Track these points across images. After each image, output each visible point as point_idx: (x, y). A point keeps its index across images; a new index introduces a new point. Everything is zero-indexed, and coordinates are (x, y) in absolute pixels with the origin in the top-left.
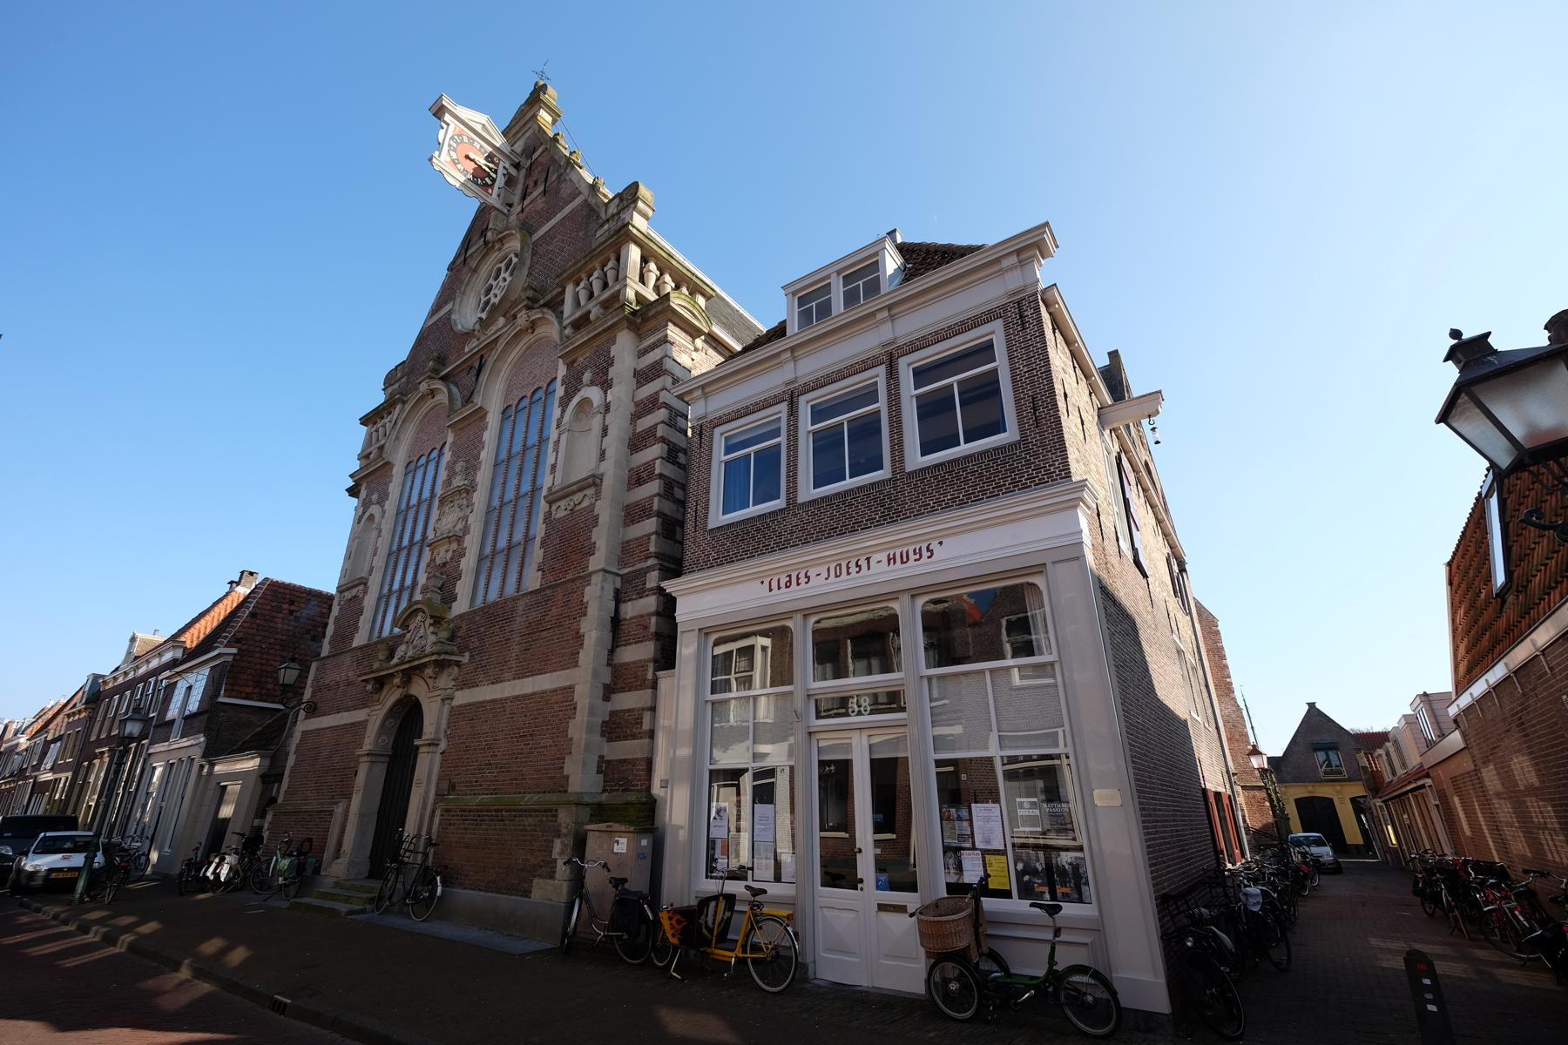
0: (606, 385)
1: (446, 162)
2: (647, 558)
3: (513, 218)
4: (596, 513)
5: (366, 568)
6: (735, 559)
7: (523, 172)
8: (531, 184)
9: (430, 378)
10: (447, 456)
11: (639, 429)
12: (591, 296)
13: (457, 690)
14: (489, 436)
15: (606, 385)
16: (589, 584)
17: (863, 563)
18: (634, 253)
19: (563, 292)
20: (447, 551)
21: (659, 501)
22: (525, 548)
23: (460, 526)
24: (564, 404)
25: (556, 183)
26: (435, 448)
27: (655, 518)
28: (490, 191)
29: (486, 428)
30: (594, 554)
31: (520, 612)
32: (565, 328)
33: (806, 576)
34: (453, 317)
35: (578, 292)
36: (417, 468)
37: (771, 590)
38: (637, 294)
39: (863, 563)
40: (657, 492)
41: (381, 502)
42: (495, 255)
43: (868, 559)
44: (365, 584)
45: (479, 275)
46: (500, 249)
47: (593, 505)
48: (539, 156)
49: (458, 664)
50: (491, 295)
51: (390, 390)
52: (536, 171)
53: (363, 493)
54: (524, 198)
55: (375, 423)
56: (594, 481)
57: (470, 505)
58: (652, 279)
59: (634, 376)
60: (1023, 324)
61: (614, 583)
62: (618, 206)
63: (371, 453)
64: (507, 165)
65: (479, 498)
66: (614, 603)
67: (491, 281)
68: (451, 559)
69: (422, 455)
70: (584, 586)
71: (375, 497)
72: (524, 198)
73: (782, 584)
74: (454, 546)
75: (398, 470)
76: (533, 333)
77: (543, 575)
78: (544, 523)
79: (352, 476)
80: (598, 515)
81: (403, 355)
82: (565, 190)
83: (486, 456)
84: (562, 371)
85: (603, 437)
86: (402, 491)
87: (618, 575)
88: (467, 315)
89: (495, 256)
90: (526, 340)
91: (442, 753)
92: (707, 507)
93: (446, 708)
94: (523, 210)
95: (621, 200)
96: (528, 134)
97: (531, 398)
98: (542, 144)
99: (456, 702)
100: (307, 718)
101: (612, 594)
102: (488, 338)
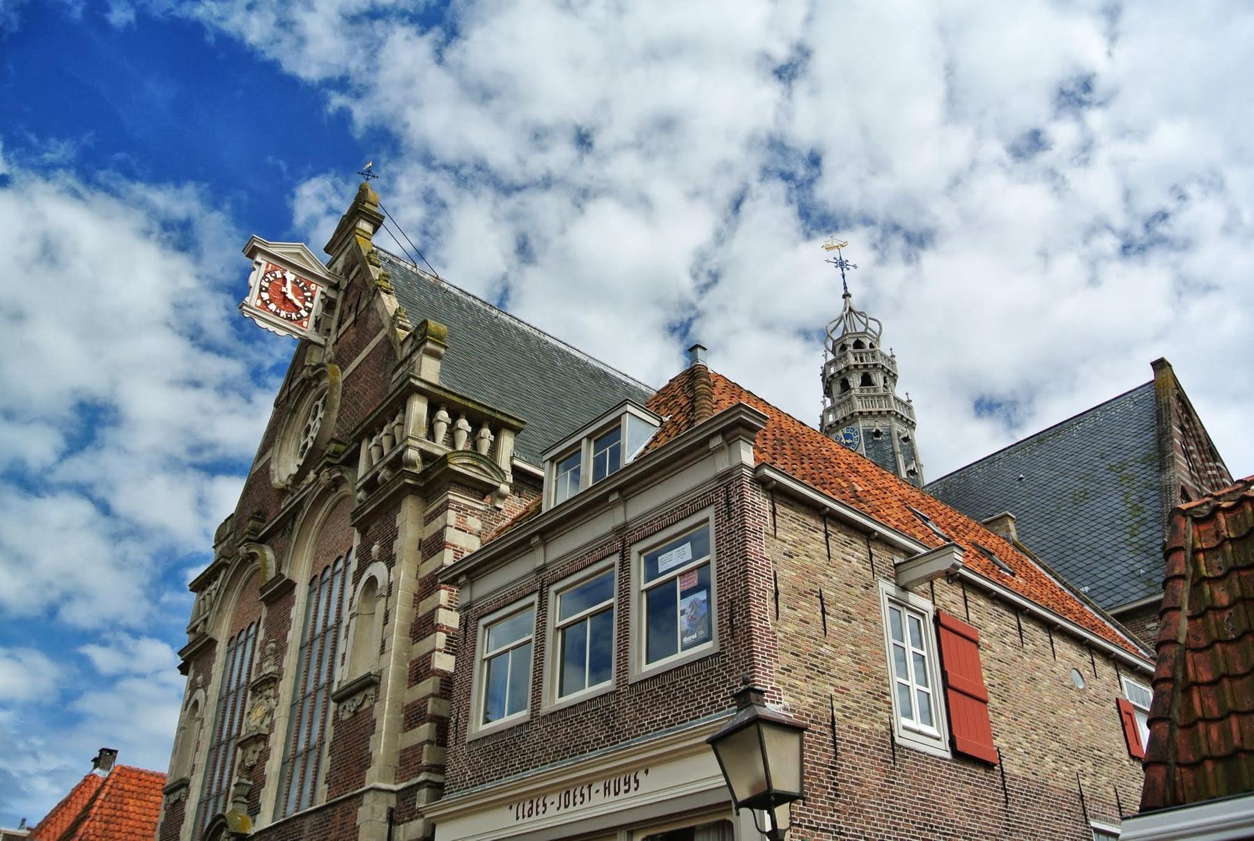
0: (390, 561)
2: (419, 773)
3: (329, 349)
4: (374, 717)
5: (189, 767)
6: (486, 780)
7: (342, 294)
8: (346, 309)
9: (248, 540)
10: (261, 636)
11: (421, 614)
12: (382, 455)
15: (390, 561)
16: (361, 805)
17: (586, 791)
18: (418, 408)
20: (254, 752)
21: (434, 702)
22: (319, 752)
23: (267, 721)
24: (356, 581)
25: (365, 311)
26: (243, 630)
27: (428, 724)
28: (305, 324)
29: (293, 604)
30: (370, 767)
31: (306, 832)
32: (358, 491)
33: (545, 805)
34: (272, 467)
35: (370, 449)
36: (237, 645)
37: (518, 818)
38: (422, 452)
39: (586, 791)
40: (431, 692)
41: (205, 685)
42: (314, 390)
43: (590, 787)
45: (299, 414)
46: (316, 386)
47: (372, 706)
48: (355, 277)
50: (309, 439)
51: (219, 548)
52: (352, 294)
53: (192, 672)
54: (339, 327)
55: (204, 589)
56: (370, 683)
57: (276, 696)
58: (441, 430)
59: (419, 549)
60: (729, 513)
61: (388, 802)
62: (412, 345)
63: (197, 626)
64: (325, 289)
65: (286, 687)
66: (387, 826)
67: (310, 422)
68: (258, 761)
69: (243, 630)
70: (358, 807)
71: (200, 678)
72: (339, 327)
73: (526, 814)
74: (261, 746)
75: (221, 648)
76: (337, 491)
77: (329, 788)
78: (333, 724)
79: (180, 653)
80: (375, 720)
82: (371, 324)
83: (294, 637)
84: (356, 541)
85: (385, 624)
86: (224, 672)
87: (392, 792)
88: (286, 466)
89: (313, 393)
90: (330, 499)
92: (467, 716)
94: (337, 340)
95: (415, 337)
96: (348, 249)
97: (322, 577)
98: (357, 263)
101: (385, 815)
102: (301, 493)
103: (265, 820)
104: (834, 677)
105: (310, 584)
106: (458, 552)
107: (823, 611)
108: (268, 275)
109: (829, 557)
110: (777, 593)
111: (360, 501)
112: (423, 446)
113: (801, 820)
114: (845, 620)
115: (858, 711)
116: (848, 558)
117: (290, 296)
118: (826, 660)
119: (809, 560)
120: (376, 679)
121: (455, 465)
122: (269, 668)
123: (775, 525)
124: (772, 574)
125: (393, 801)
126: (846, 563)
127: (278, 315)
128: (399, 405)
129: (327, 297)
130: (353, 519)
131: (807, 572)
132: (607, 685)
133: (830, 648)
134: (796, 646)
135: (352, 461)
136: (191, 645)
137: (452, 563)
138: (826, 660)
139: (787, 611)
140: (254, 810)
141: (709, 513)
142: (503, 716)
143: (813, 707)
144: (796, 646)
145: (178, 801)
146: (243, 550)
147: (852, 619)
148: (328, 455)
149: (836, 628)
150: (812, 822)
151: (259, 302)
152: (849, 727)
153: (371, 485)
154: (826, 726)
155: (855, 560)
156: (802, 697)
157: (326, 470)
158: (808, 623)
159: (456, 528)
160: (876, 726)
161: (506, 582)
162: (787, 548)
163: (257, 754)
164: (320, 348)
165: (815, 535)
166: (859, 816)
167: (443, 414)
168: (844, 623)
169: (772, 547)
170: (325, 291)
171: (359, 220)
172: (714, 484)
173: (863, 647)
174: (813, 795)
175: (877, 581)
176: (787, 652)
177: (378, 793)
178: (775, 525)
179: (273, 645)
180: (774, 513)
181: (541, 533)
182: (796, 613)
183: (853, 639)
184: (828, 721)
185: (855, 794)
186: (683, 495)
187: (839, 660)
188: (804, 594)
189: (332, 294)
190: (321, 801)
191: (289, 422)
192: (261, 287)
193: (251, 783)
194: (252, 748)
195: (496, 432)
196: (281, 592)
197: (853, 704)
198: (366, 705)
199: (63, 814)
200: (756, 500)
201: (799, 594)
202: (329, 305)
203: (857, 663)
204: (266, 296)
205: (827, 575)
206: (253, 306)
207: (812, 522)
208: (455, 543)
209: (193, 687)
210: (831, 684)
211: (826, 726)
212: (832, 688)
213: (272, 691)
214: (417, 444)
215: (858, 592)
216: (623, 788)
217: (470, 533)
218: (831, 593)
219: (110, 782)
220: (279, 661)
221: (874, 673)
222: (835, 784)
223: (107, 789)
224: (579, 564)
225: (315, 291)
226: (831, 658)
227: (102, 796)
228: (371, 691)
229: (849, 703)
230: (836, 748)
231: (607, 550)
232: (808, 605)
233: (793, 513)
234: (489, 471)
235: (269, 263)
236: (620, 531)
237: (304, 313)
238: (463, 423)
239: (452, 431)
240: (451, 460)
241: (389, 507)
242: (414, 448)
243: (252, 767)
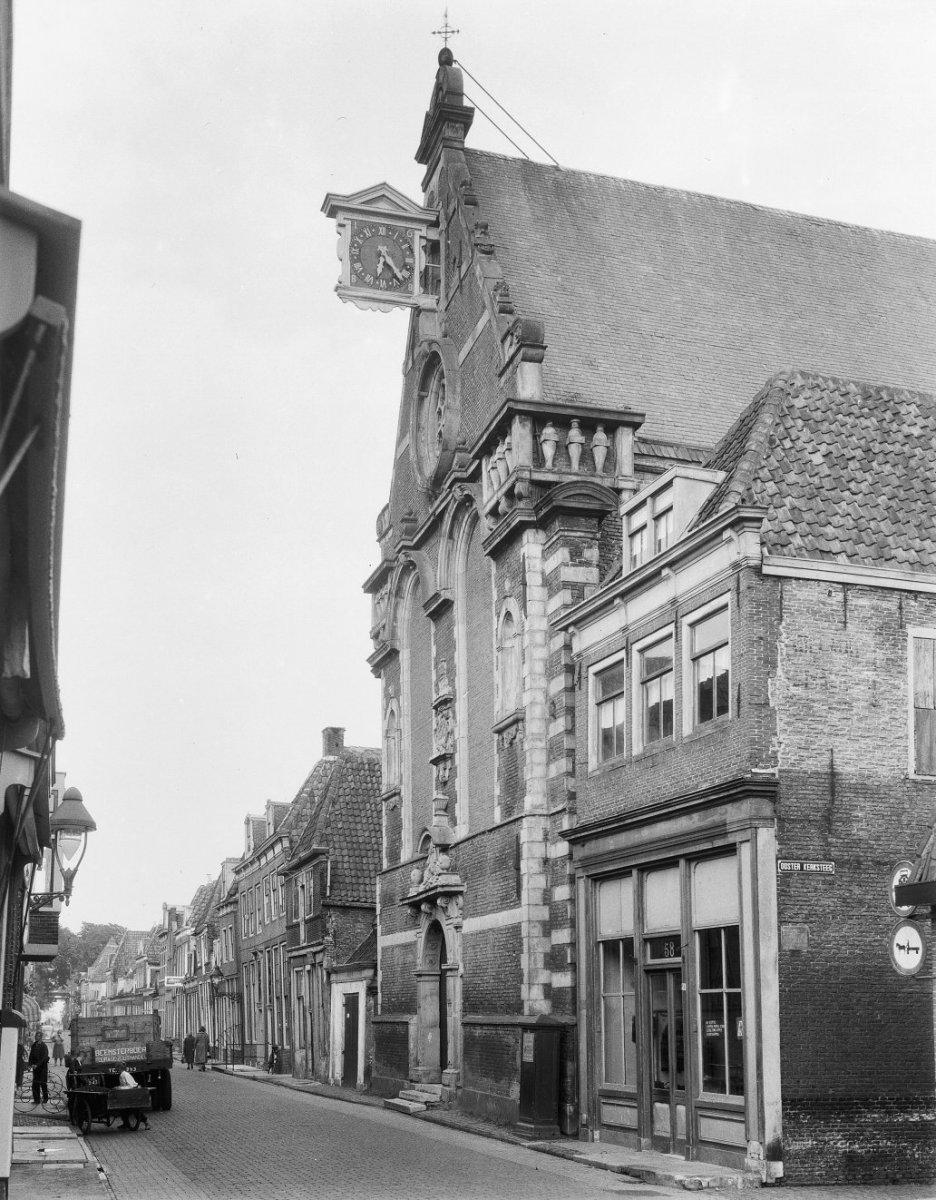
19: (480, 465)
20: (445, 769)
23: (450, 741)
38: (535, 483)
44: (399, 794)
51: (383, 541)
64: (424, 231)
65: (461, 706)
74: (449, 764)
79: (369, 660)
81: (384, 497)
103: (461, 832)
106: (577, 589)
122: (445, 691)
128: (502, 431)
129: (428, 240)
135: (476, 476)
136: (378, 652)
140: (454, 821)
141: (727, 598)
146: (402, 557)
153: (494, 512)
163: (447, 771)
170: (424, 233)
179: (445, 665)
181: (622, 595)
189: (433, 235)
194: (441, 766)
196: (440, 610)
202: (433, 248)
204: (358, 266)
209: (388, 697)
220: (452, 682)
238: (575, 434)
241: (514, 536)
243: (445, 783)
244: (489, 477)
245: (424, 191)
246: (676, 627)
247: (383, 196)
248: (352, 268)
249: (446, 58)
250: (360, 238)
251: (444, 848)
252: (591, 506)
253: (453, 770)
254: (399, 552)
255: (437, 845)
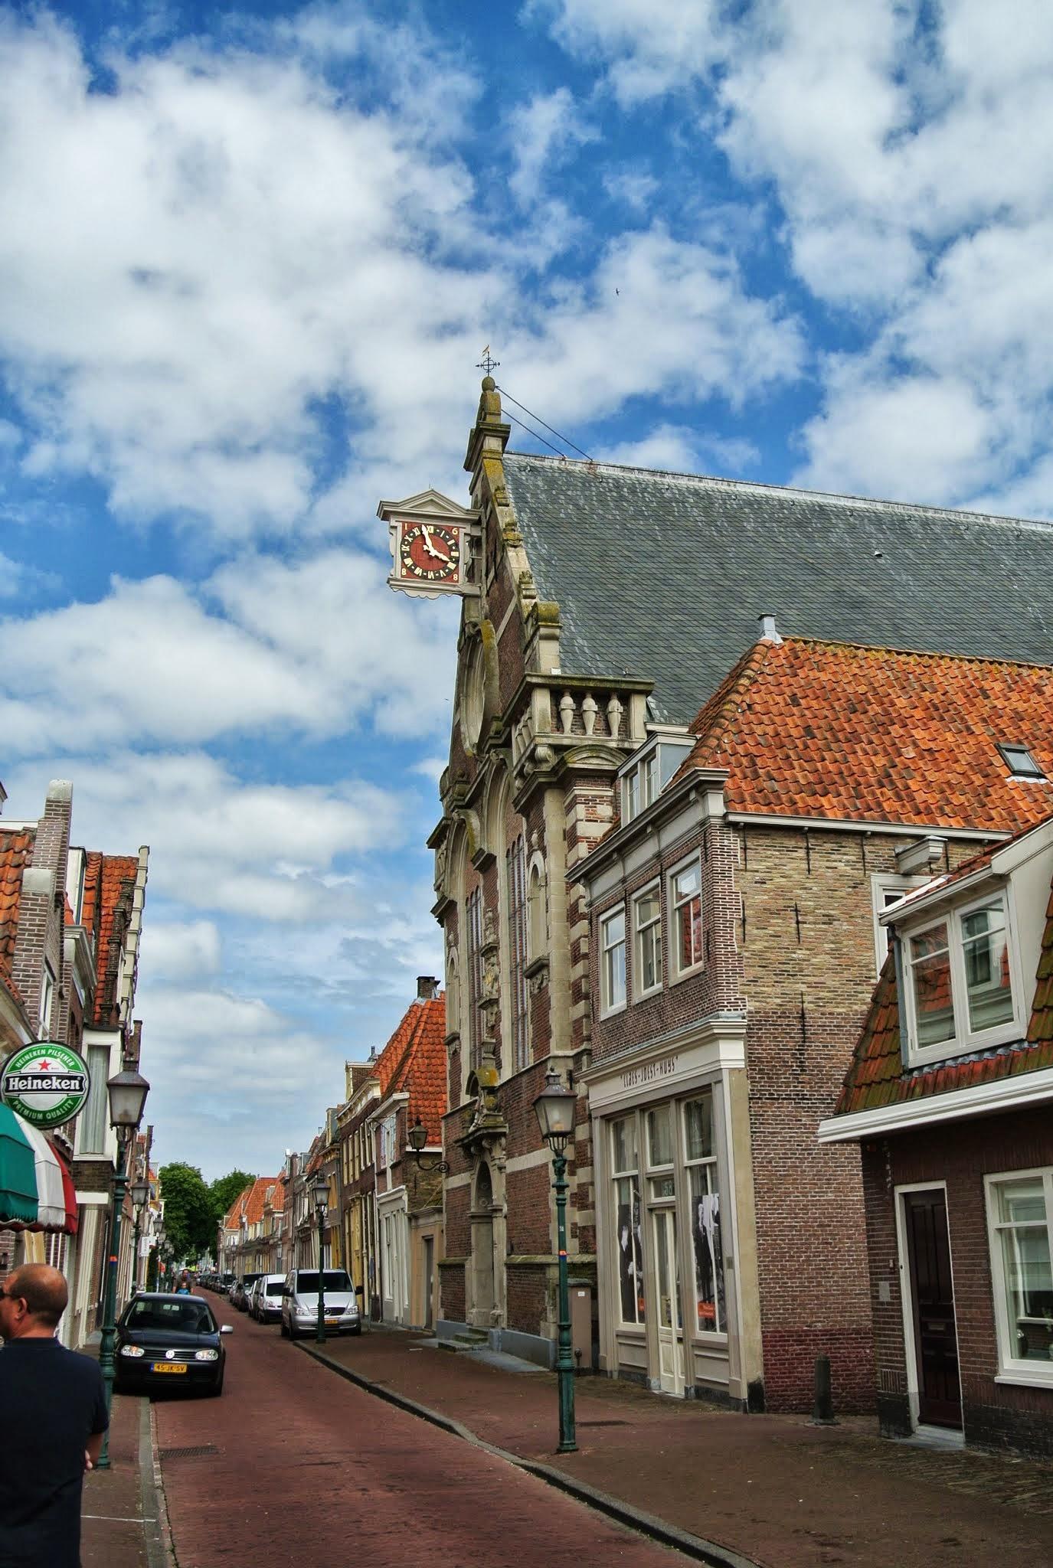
1: (402, 576)
2: (582, 1043)
13: (507, 1159)
14: (501, 883)
23: (496, 987)
28: (455, 577)
38: (551, 746)
44: (459, 1038)
49: (504, 1134)
58: (568, 717)
59: (565, 839)
64: (468, 529)
65: (504, 953)
87: (568, 1057)
88: (473, 733)
91: (505, 1217)
93: (504, 1175)
94: (488, 591)
99: (509, 1170)
100: (447, 1177)
103: (507, 1074)
104: (809, 976)
105: (507, 857)
107: (798, 922)
108: (407, 538)
109: (809, 870)
110: (744, 921)
111: (518, 789)
112: (551, 741)
113: (761, 1094)
114: (824, 923)
115: (834, 999)
116: (834, 864)
117: (433, 552)
118: (798, 964)
119: (784, 880)
120: (545, 962)
121: (574, 763)
123: (746, 860)
124: (741, 904)
125: (571, 1065)
126: (830, 870)
127: (426, 578)
128: (524, 701)
130: (516, 807)
131: (781, 892)
132: (658, 987)
133: (804, 952)
134: (764, 959)
135: (507, 744)
137: (587, 855)
138: (798, 964)
139: (755, 931)
142: (691, 964)
143: (781, 1005)
144: (764, 959)
145: (455, 1051)
147: (835, 920)
148: (491, 738)
149: (812, 933)
150: (773, 1094)
151: (404, 572)
152: (822, 1014)
154: (795, 1018)
155: (843, 864)
156: (768, 1000)
157: (493, 751)
158: (780, 936)
159: (587, 821)
160: (855, 1007)
161: (604, 890)
162: (758, 877)
164: (476, 600)
165: (794, 854)
166: (827, 1083)
167: (567, 701)
168: (823, 926)
169: (742, 881)
170: (469, 532)
171: (484, 439)
172: (698, 830)
173: (845, 943)
174: (777, 1074)
175: (869, 877)
176: (754, 966)
177: (557, 1060)
178: (746, 860)
179: (490, 914)
180: (745, 849)
182: (767, 931)
183: (832, 938)
184: (798, 1013)
185: (824, 1067)
186: (682, 836)
187: (814, 960)
188: (777, 913)
189: (476, 532)
190: (531, 1063)
191: (468, 679)
192: (402, 553)
193: (494, 1041)
195: (625, 700)
197: (828, 994)
198: (544, 984)
199: (395, 1048)
200: (726, 842)
201: (771, 914)
203: (836, 958)
204: (409, 561)
205: (805, 888)
206: (399, 577)
207: (791, 843)
208: (587, 835)
210: (803, 983)
211: (795, 1018)
212: (805, 986)
213: (495, 958)
214: (545, 740)
215: (843, 894)
216: (668, 1068)
217: (601, 822)
218: (810, 903)
219: (424, 1019)
220: (496, 933)
221: (857, 962)
222: (801, 1062)
223: (423, 1024)
224: (685, 851)
225: (458, 536)
226: (804, 960)
227: (419, 1033)
228: (545, 972)
229: (822, 994)
230: (804, 1033)
231: (651, 874)
232: (780, 921)
233: (768, 842)
234: (609, 758)
235: (404, 523)
236: (658, 856)
237: (452, 566)
238: (590, 704)
239: (579, 714)
240: (570, 760)
242: (543, 745)
243: (493, 1027)
244: (517, 741)
245: (471, 494)
246: (661, 879)
247: (432, 500)
248: (403, 562)
249: (488, 386)
250: (410, 537)
251: (492, 1091)
252: (606, 768)
253: (498, 1016)
254: (453, 811)
255: (483, 1088)
